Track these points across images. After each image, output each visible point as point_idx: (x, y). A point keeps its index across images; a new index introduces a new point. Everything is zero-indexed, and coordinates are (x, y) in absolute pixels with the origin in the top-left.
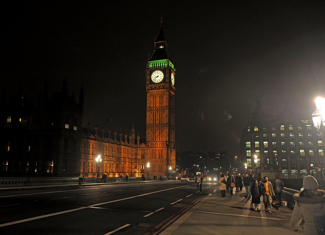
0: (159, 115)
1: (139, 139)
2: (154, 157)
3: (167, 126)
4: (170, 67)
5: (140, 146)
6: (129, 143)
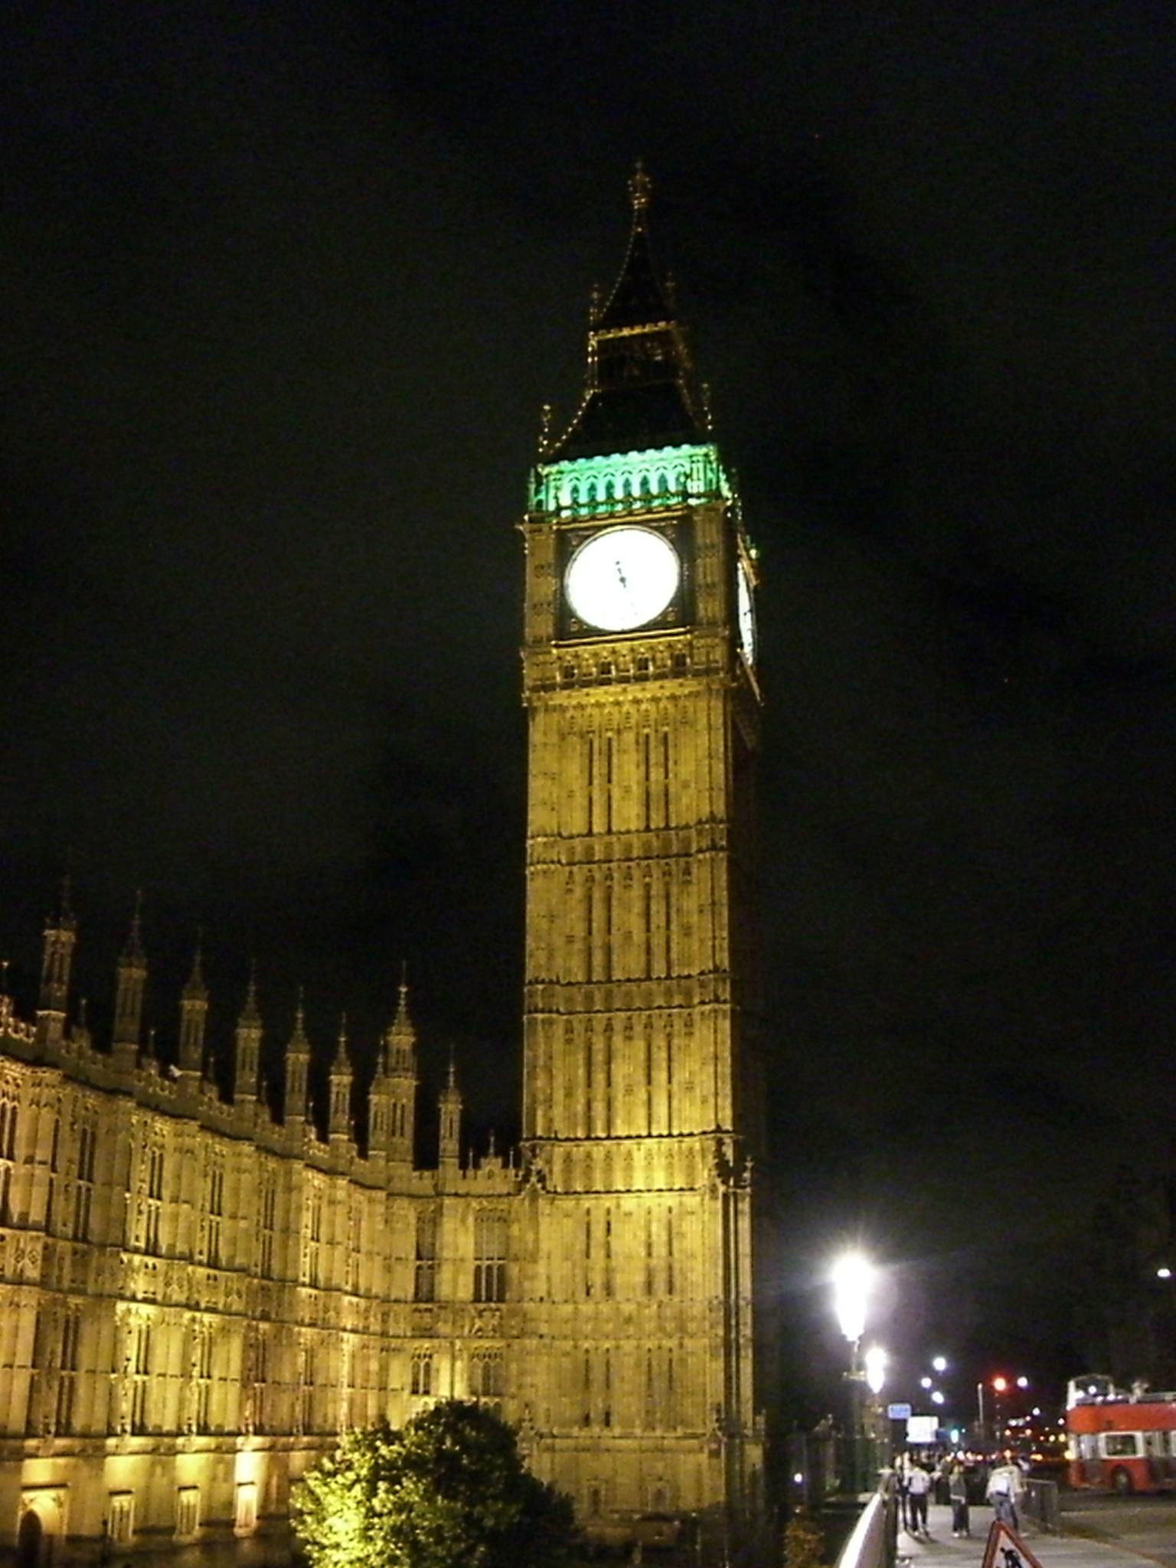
0: (638, 907)
1: (456, 1118)
2: (597, 1279)
6: (363, 1154)
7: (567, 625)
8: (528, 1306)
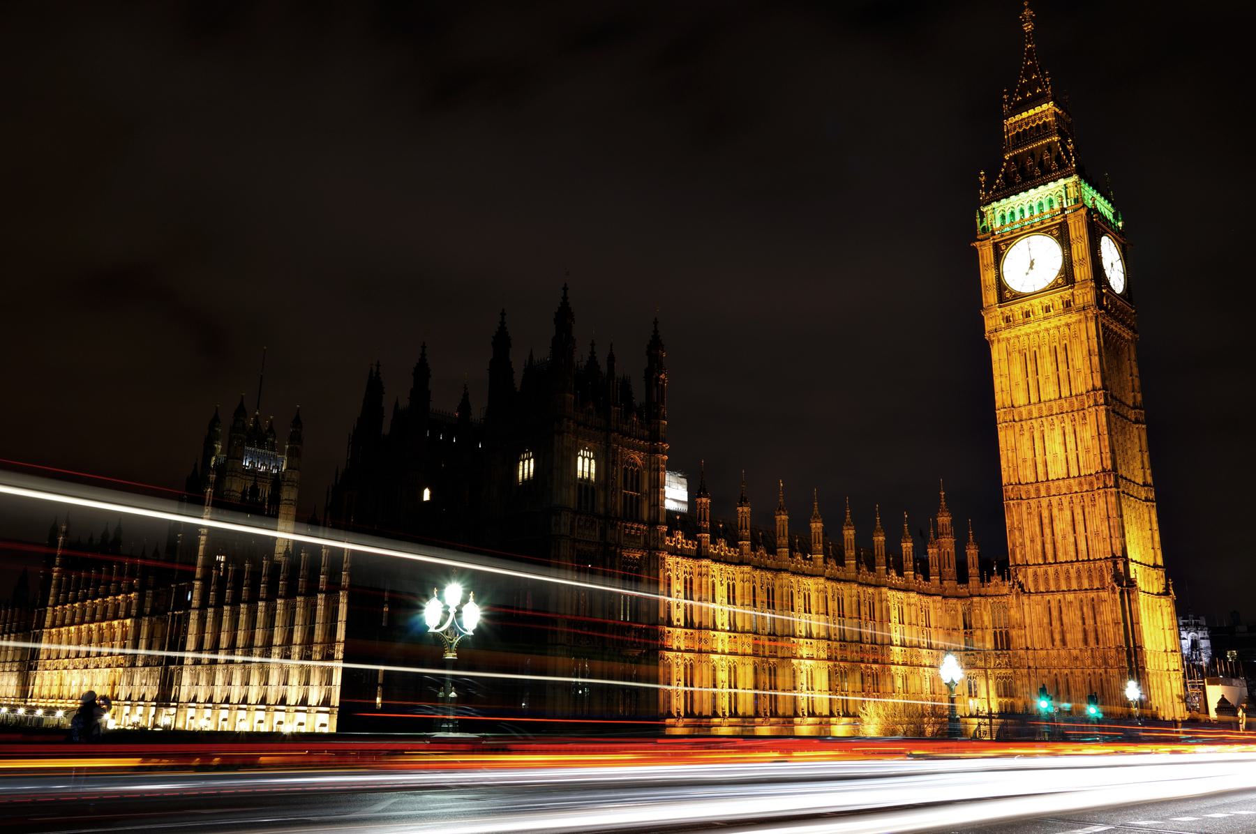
0: (1059, 439)
2: (1057, 637)
3: (1106, 487)
4: (1089, 210)
5: (983, 591)
7: (1005, 295)
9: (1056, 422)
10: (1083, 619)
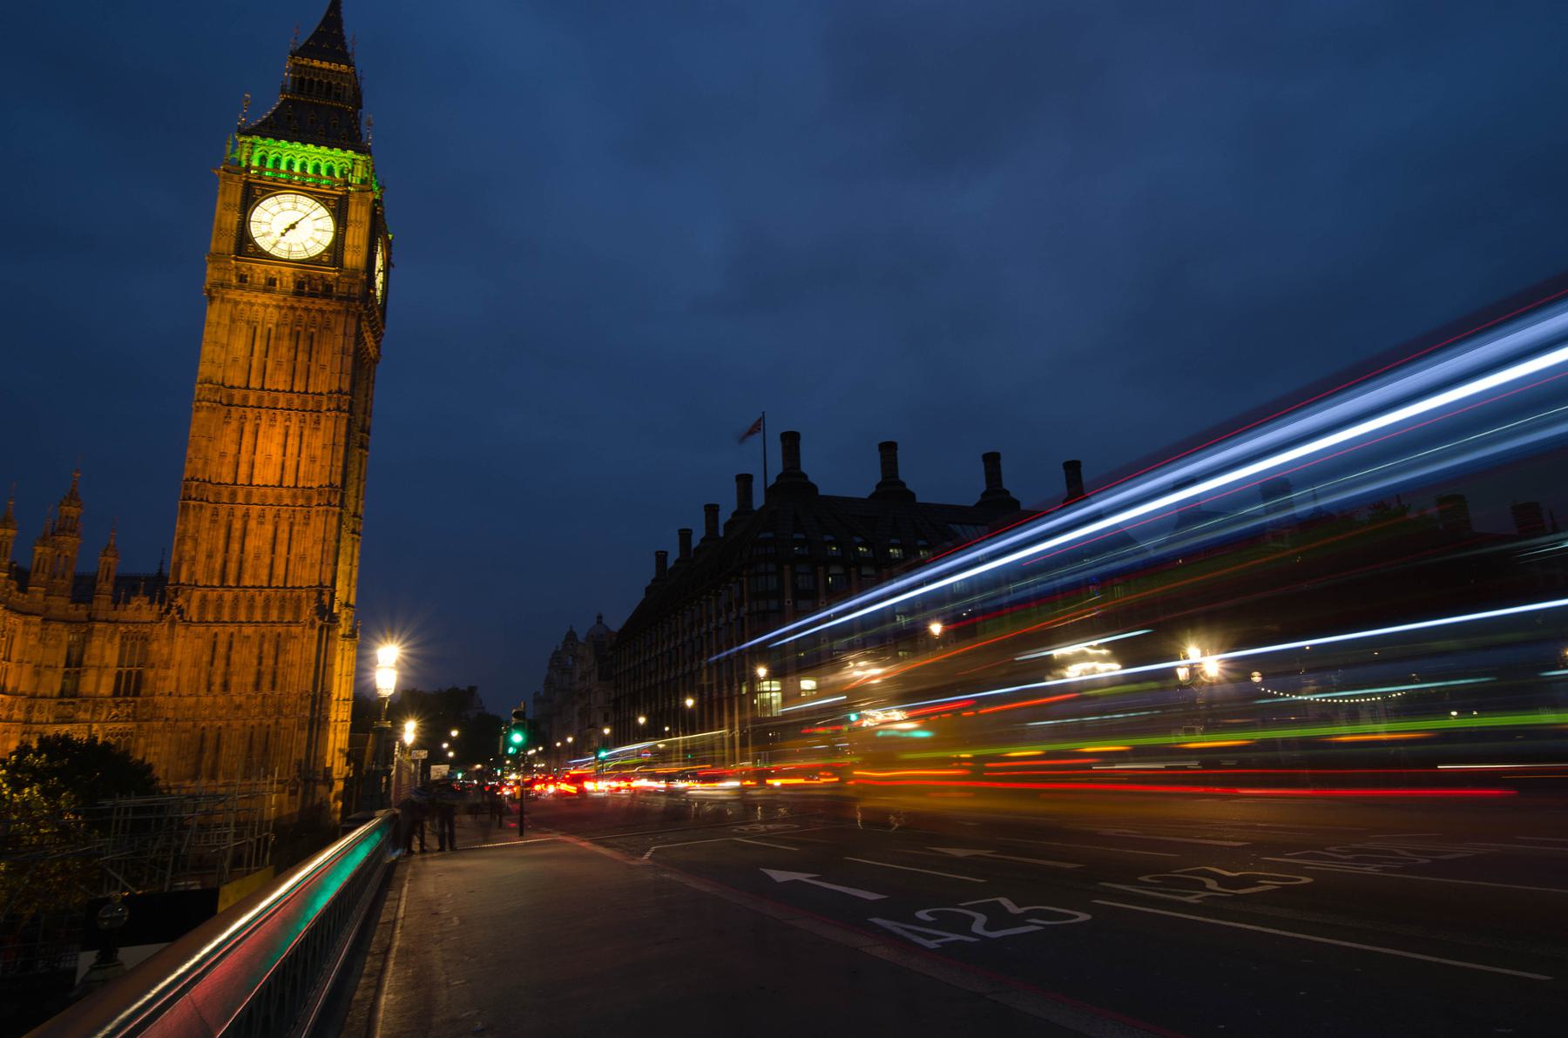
0: (279, 439)
3: (329, 504)
5: (114, 615)
8: (158, 699)
9: (279, 418)
10: (260, 659)
